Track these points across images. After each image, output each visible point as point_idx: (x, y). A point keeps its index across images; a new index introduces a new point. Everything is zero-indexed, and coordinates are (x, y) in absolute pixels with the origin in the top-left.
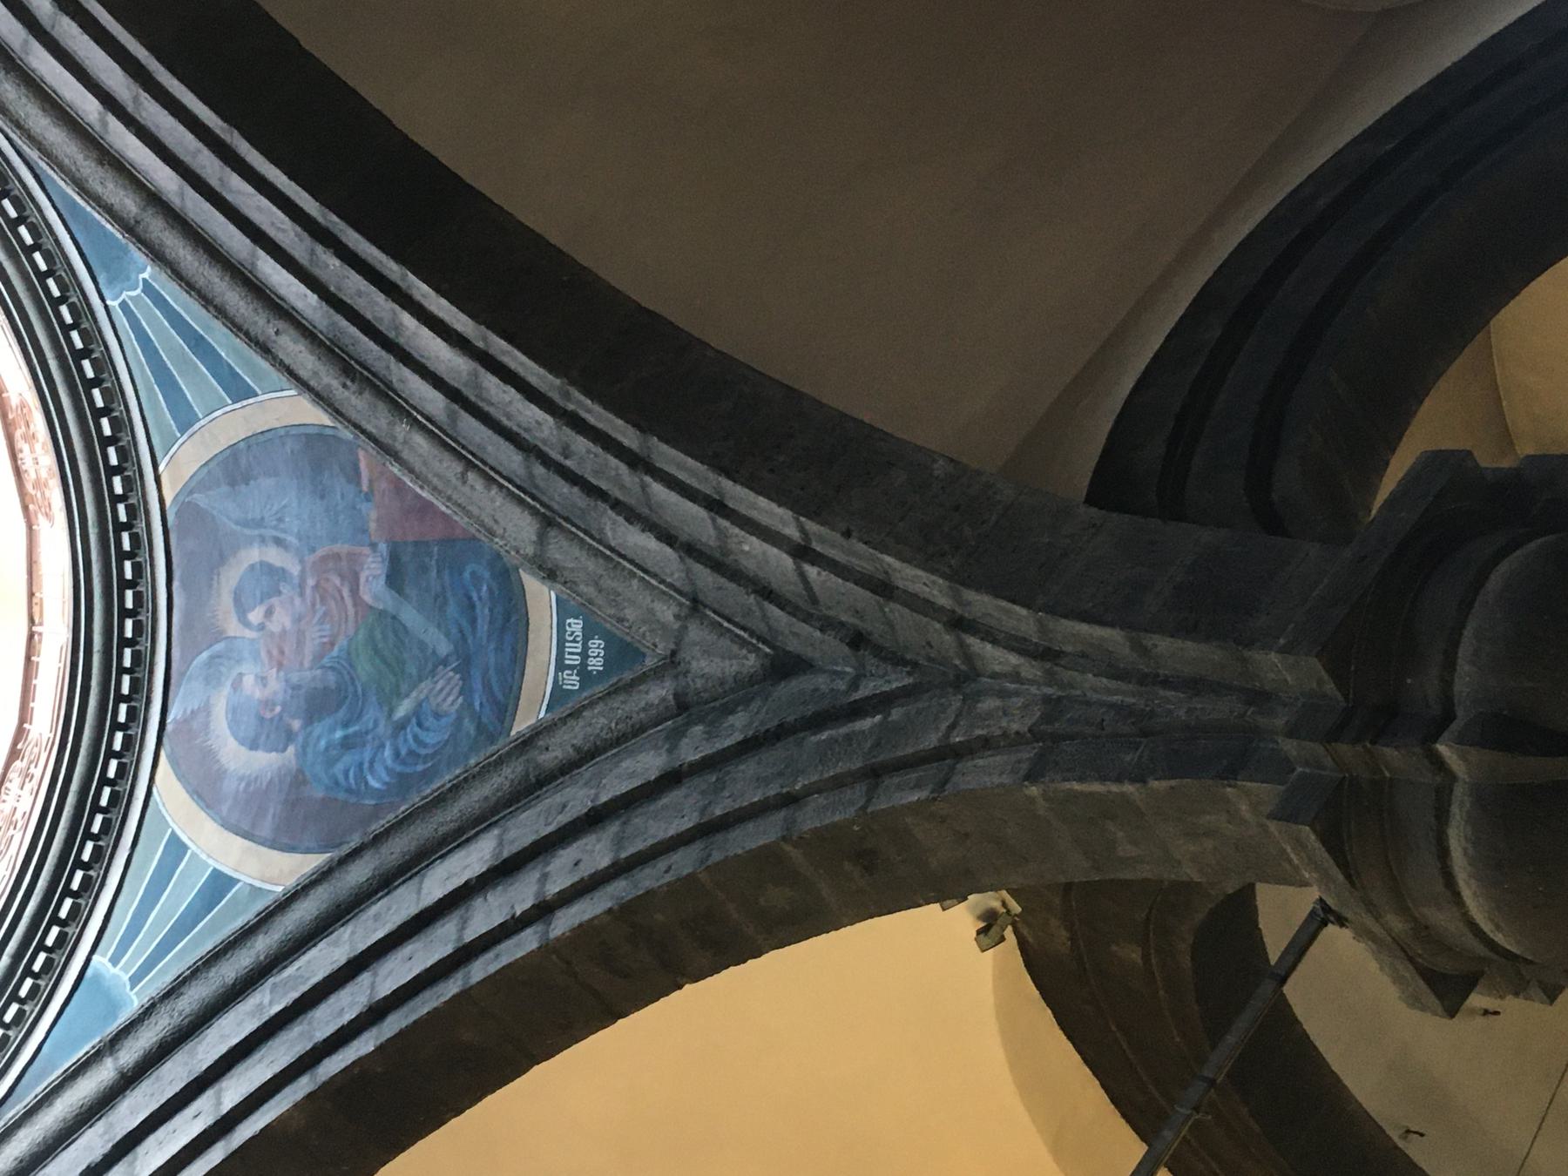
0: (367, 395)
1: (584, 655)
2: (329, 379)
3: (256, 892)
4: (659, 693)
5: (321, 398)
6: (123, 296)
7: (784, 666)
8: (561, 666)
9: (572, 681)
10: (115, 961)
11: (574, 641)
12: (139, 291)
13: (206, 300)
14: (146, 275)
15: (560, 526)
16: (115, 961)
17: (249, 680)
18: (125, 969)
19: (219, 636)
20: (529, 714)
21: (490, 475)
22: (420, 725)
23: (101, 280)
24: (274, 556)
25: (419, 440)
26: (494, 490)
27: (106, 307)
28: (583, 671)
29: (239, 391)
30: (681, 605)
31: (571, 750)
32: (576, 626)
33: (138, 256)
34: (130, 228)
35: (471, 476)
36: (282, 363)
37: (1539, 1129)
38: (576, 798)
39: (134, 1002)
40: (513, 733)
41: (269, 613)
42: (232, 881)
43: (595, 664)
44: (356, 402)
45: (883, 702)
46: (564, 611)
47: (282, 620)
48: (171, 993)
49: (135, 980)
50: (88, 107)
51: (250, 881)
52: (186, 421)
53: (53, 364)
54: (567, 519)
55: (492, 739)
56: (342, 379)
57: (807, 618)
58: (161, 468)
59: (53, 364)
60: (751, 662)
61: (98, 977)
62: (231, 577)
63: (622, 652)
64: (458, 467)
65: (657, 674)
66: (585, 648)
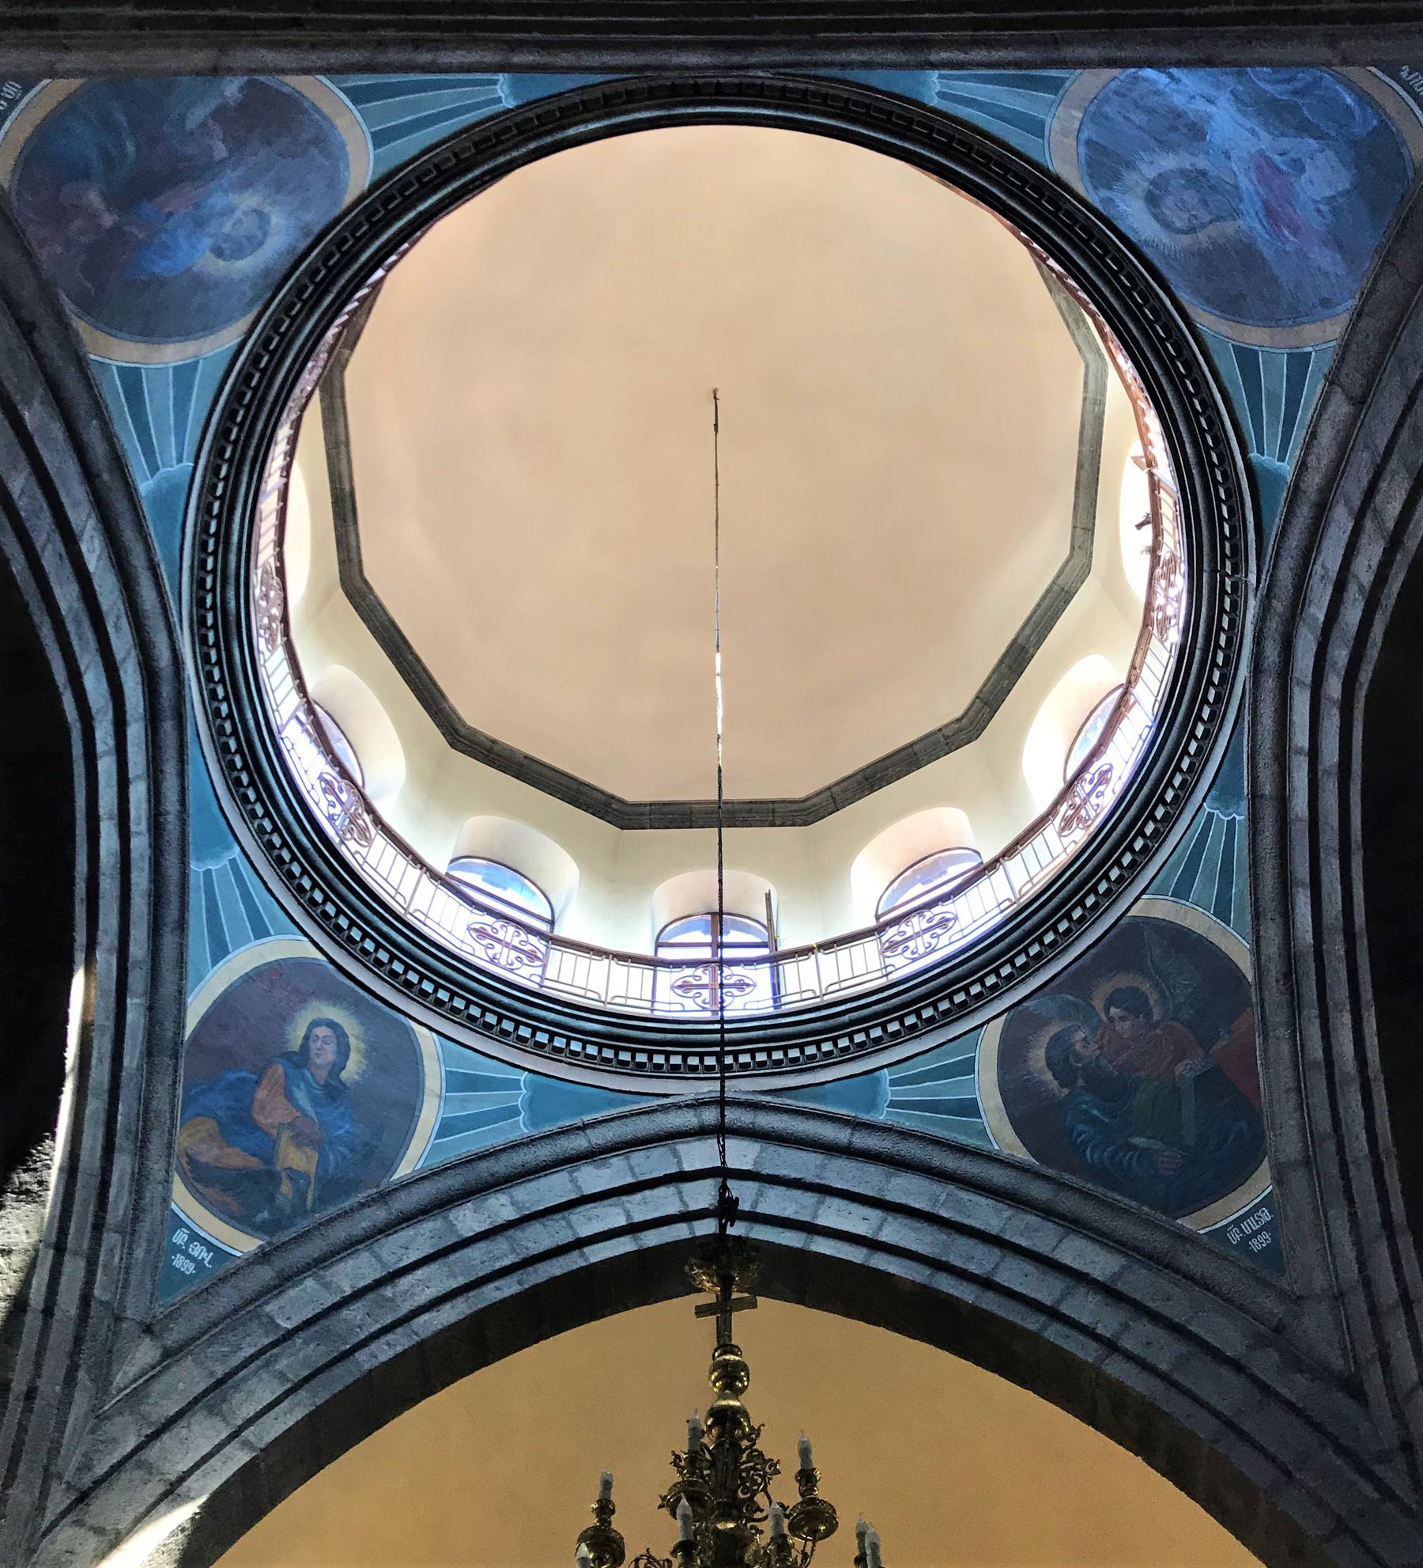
0: (1285, 998)
1: (1255, 1234)
2: (1274, 969)
3: (982, 1133)
4: (1274, 1308)
5: (1258, 966)
6: (1216, 812)
7: (1354, 1388)
8: (1237, 1222)
9: (1235, 1237)
10: (893, 1083)
11: (1257, 1222)
12: (1226, 819)
13: (1254, 864)
14: (1238, 818)
15: (1310, 1171)
16: (893, 1083)
17: (1080, 1035)
19: (1087, 998)
20: (1196, 1224)
21: (1303, 1107)
22: (1139, 1157)
23: (1213, 792)
24: (1153, 998)
25: (1285, 1048)
26: (1297, 1115)
27: (1201, 805)
28: (1246, 1239)
29: (1222, 912)
30: (1331, 1287)
31: (1199, 1274)
32: (1266, 1216)
33: (1244, 805)
34: (1255, 796)
35: (1293, 1095)
36: (1258, 931)
38: (1178, 1305)
39: (882, 1117)
40: (1179, 1221)
41: (1122, 1019)
43: (1256, 1245)
44: (1275, 994)
45: (1388, 1494)
47: (1125, 1028)
48: (905, 1135)
49: (892, 1104)
50: (1301, 737)
51: (986, 1125)
52: (1181, 892)
53: (1145, 790)
54: (1318, 1174)
55: (1165, 1213)
56: (1280, 977)
57: (1393, 1400)
58: (1144, 896)
59: (1145, 790)
60: (1338, 1363)
61: (878, 1080)
62: (1123, 981)
63: (1273, 1257)
64: (1292, 1084)
65: (1283, 1296)
66: (1259, 1231)
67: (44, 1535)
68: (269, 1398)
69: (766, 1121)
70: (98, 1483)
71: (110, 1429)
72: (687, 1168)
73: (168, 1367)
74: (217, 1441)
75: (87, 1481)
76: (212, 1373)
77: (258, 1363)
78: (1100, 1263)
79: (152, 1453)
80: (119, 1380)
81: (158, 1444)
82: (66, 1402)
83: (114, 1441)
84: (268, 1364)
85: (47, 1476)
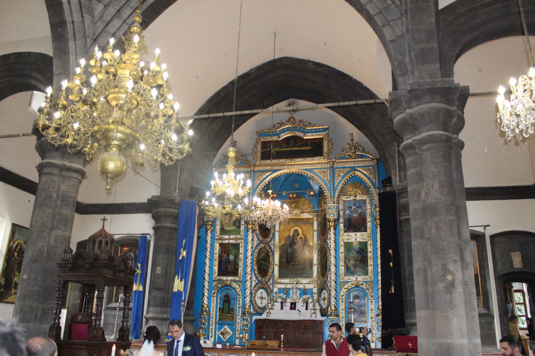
67: (89, 49)
68: (130, 13)
70: (97, 37)
71: (97, 25)
73: (106, 9)
74: (120, 24)
75: (95, 37)
76: (116, 9)
77: (126, 5)
79: (107, 29)
80: (96, 14)
81: (108, 27)
82: (83, 22)
83: (98, 27)
84: (129, 5)
85: (85, 37)
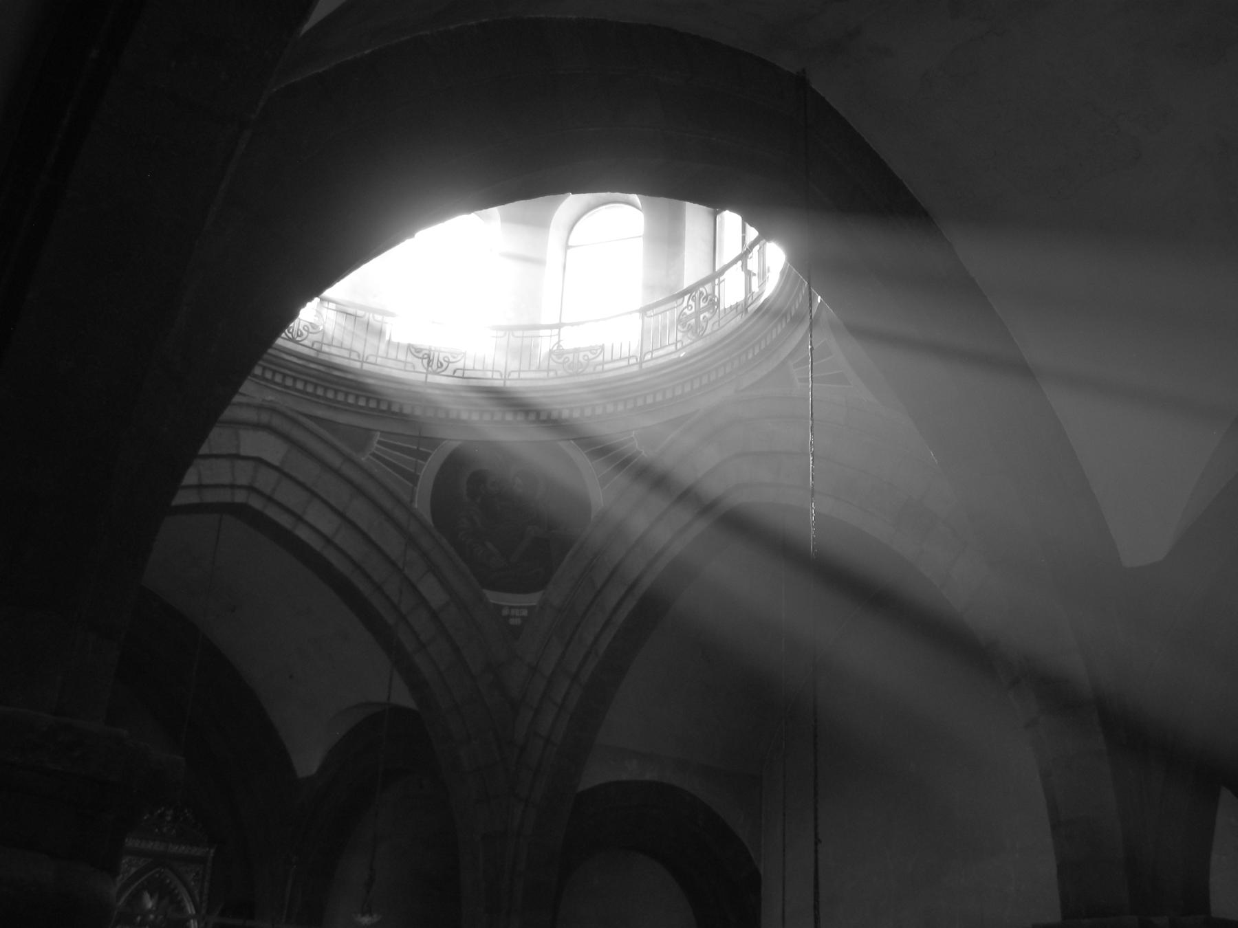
1: (515, 617)
8: (511, 607)
9: (505, 612)
10: (379, 442)
16: (379, 442)
18: (377, 449)
20: (493, 597)
28: (509, 617)
32: (525, 613)
37: (365, 346)
39: (363, 459)
40: (485, 591)
42: (415, 484)
43: (512, 622)
46: (530, 609)
48: (371, 476)
49: (374, 455)
69: (297, 434)
72: (243, 452)
78: (434, 594)
